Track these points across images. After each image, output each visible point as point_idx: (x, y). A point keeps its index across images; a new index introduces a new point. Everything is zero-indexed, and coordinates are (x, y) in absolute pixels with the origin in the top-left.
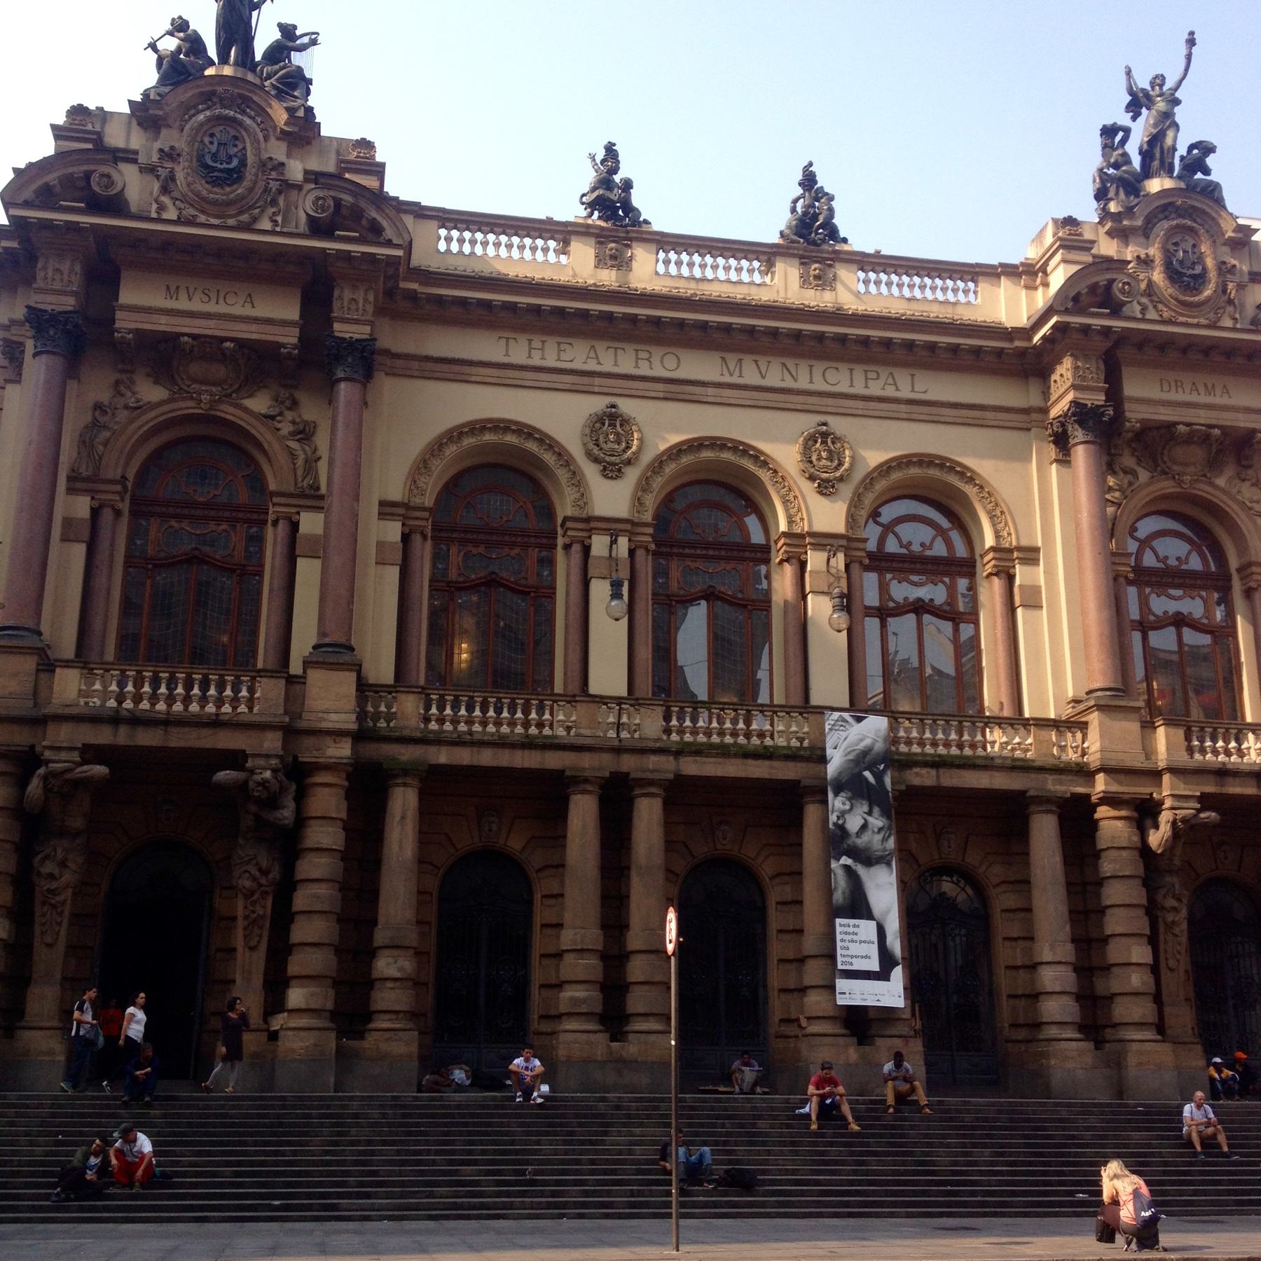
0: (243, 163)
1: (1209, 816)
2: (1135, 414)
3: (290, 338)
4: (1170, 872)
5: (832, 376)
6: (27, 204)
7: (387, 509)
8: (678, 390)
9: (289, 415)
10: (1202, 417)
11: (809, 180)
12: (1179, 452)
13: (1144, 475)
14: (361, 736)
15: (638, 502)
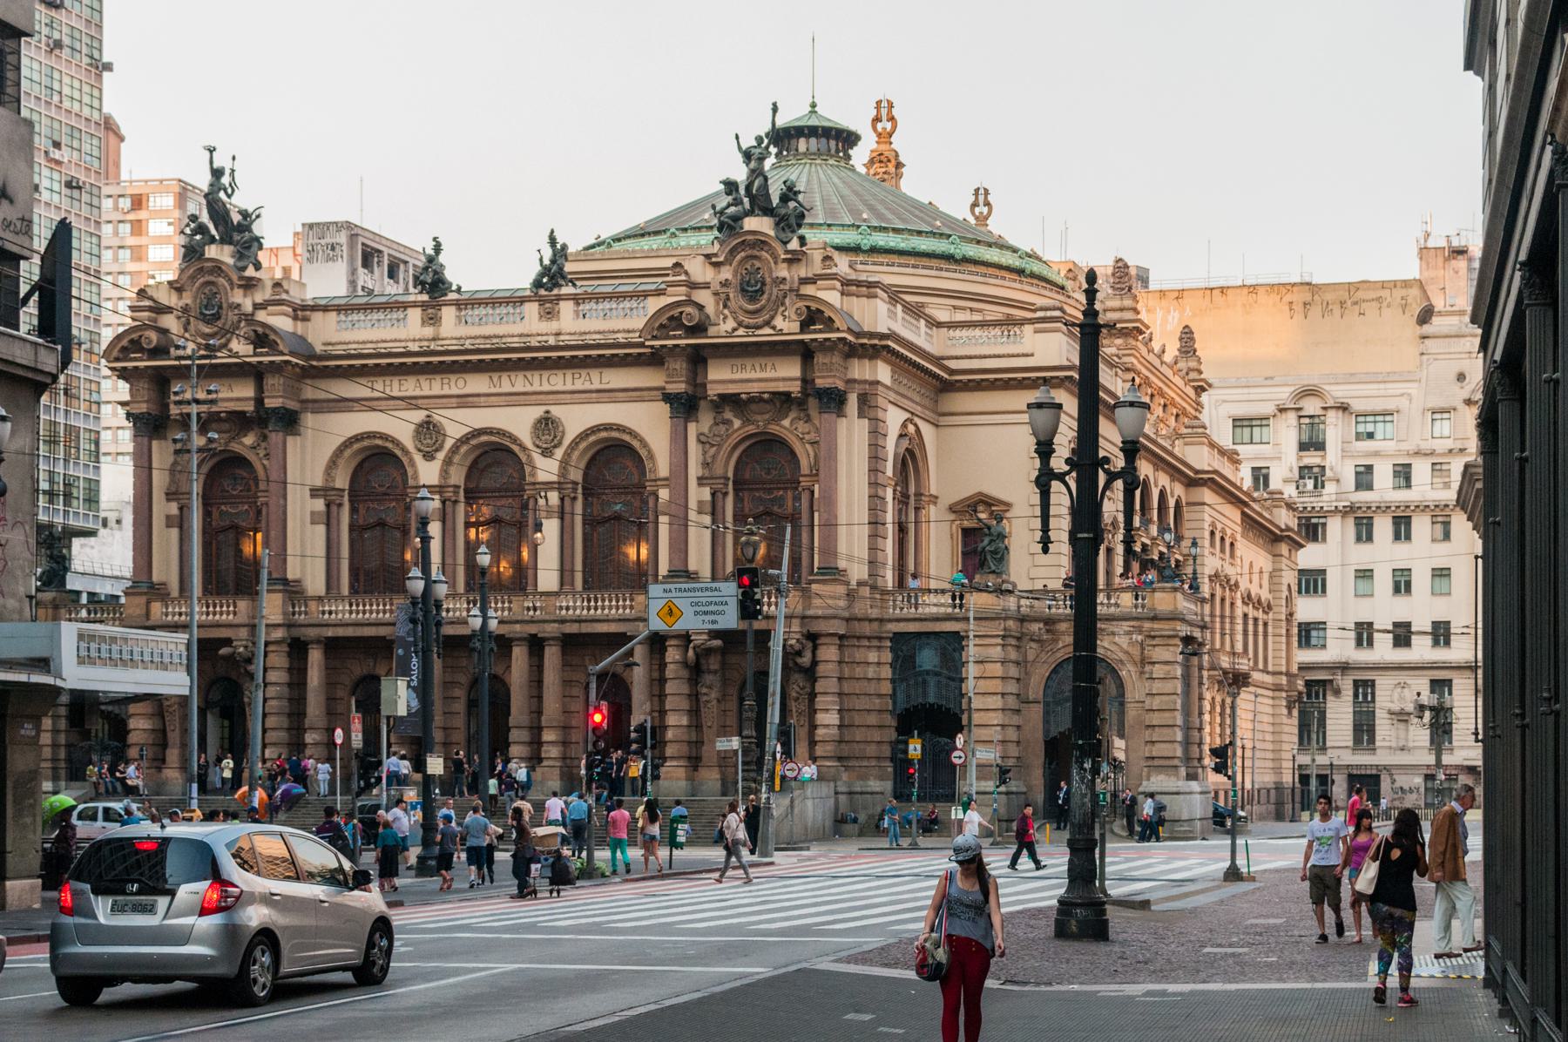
0: (220, 307)
1: (717, 643)
2: (713, 391)
3: (249, 407)
4: (710, 672)
5: (553, 379)
6: (117, 360)
7: (315, 493)
8: (464, 401)
9: (263, 445)
10: (755, 388)
11: (553, 241)
12: (753, 407)
13: (737, 423)
14: (289, 626)
15: (444, 473)
